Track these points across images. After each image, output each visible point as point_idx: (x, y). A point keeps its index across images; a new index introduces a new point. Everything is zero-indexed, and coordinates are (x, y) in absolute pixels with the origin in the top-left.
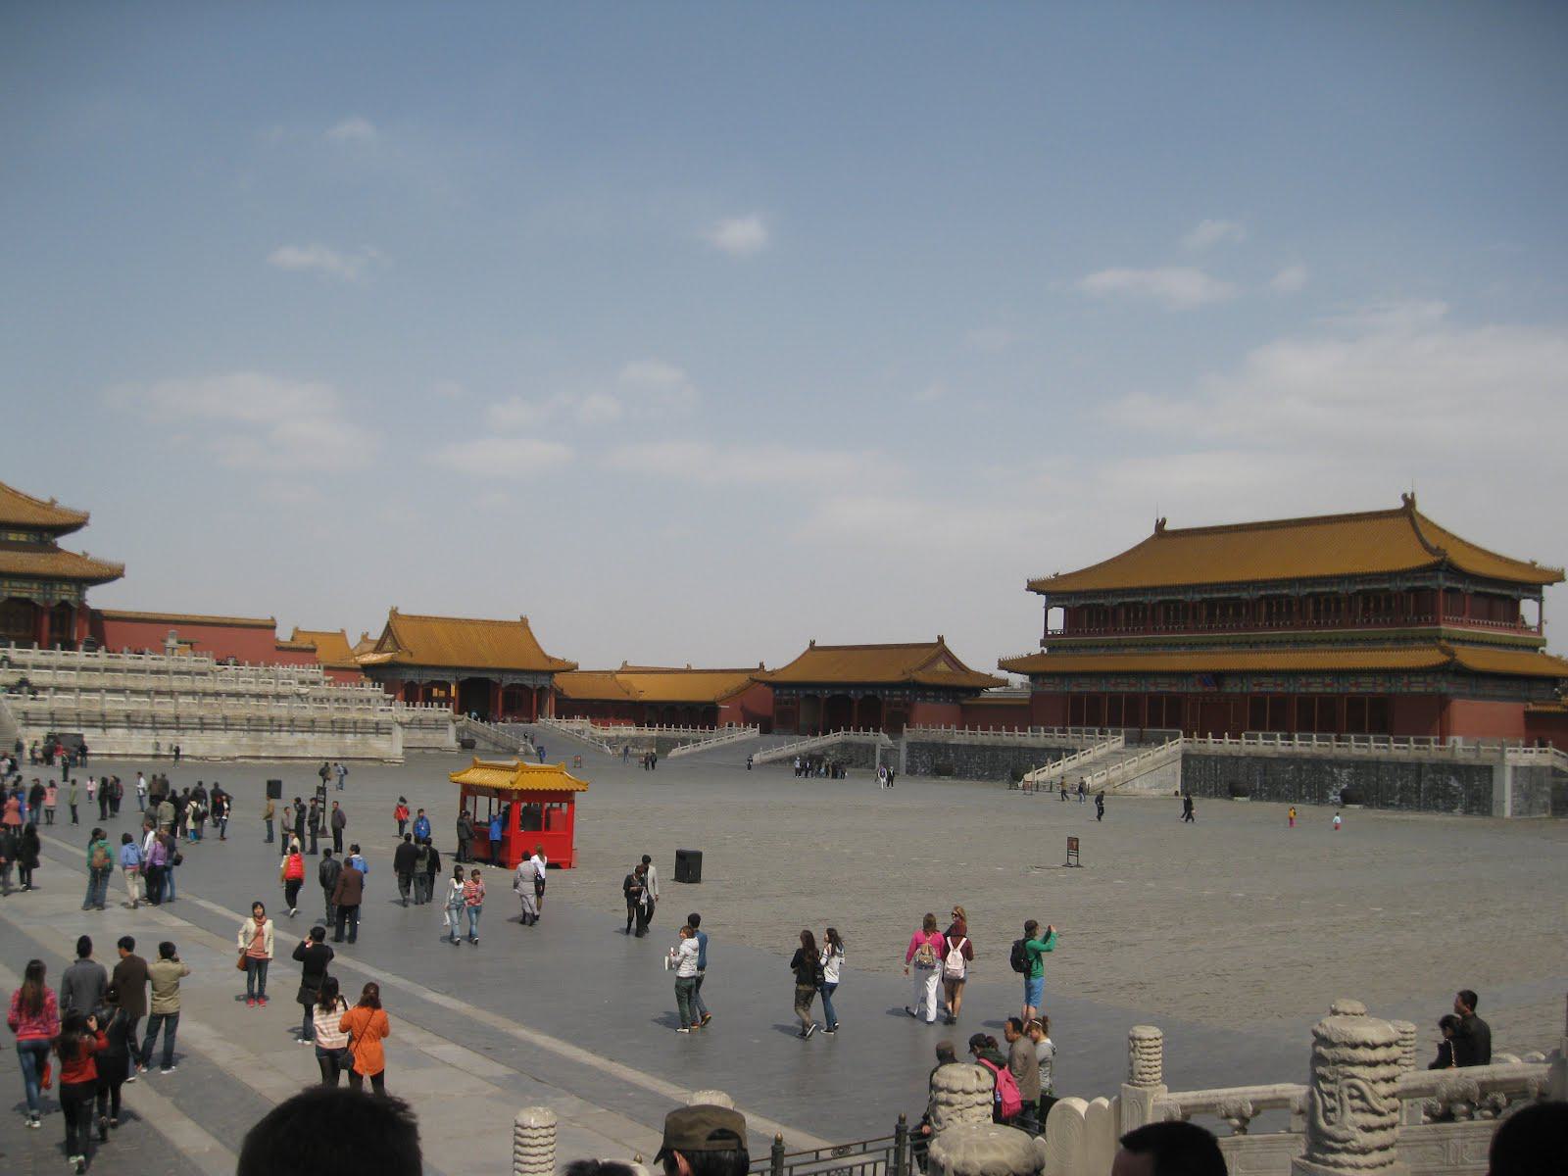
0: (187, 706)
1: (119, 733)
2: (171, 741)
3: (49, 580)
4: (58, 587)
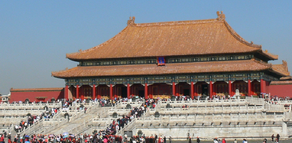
0: (199, 120)
1: (175, 129)
2: (194, 133)
4: (252, 75)
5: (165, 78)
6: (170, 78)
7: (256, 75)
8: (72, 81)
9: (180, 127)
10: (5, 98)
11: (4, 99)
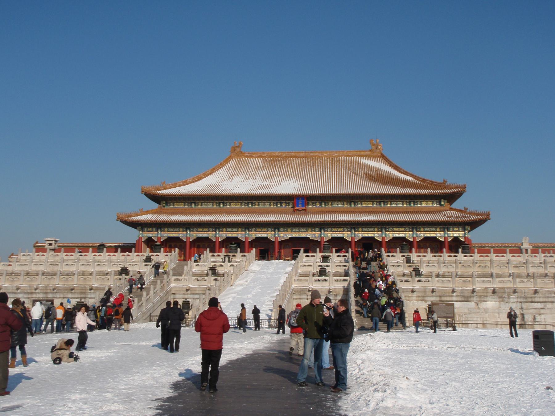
3: (445, 225)
5: (310, 230)
6: (317, 229)
7: (457, 229)
8: (150, 229)
9: (501, 300)
10: (53, 242)
11: (50, 244)
